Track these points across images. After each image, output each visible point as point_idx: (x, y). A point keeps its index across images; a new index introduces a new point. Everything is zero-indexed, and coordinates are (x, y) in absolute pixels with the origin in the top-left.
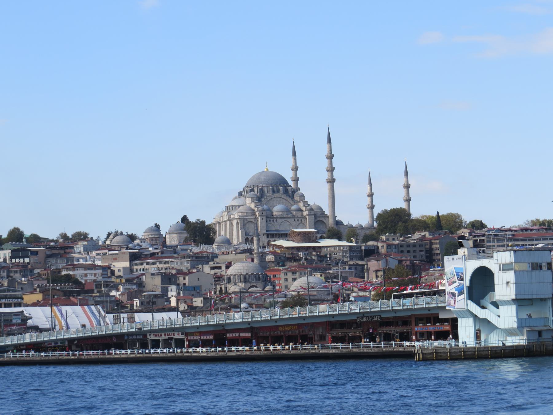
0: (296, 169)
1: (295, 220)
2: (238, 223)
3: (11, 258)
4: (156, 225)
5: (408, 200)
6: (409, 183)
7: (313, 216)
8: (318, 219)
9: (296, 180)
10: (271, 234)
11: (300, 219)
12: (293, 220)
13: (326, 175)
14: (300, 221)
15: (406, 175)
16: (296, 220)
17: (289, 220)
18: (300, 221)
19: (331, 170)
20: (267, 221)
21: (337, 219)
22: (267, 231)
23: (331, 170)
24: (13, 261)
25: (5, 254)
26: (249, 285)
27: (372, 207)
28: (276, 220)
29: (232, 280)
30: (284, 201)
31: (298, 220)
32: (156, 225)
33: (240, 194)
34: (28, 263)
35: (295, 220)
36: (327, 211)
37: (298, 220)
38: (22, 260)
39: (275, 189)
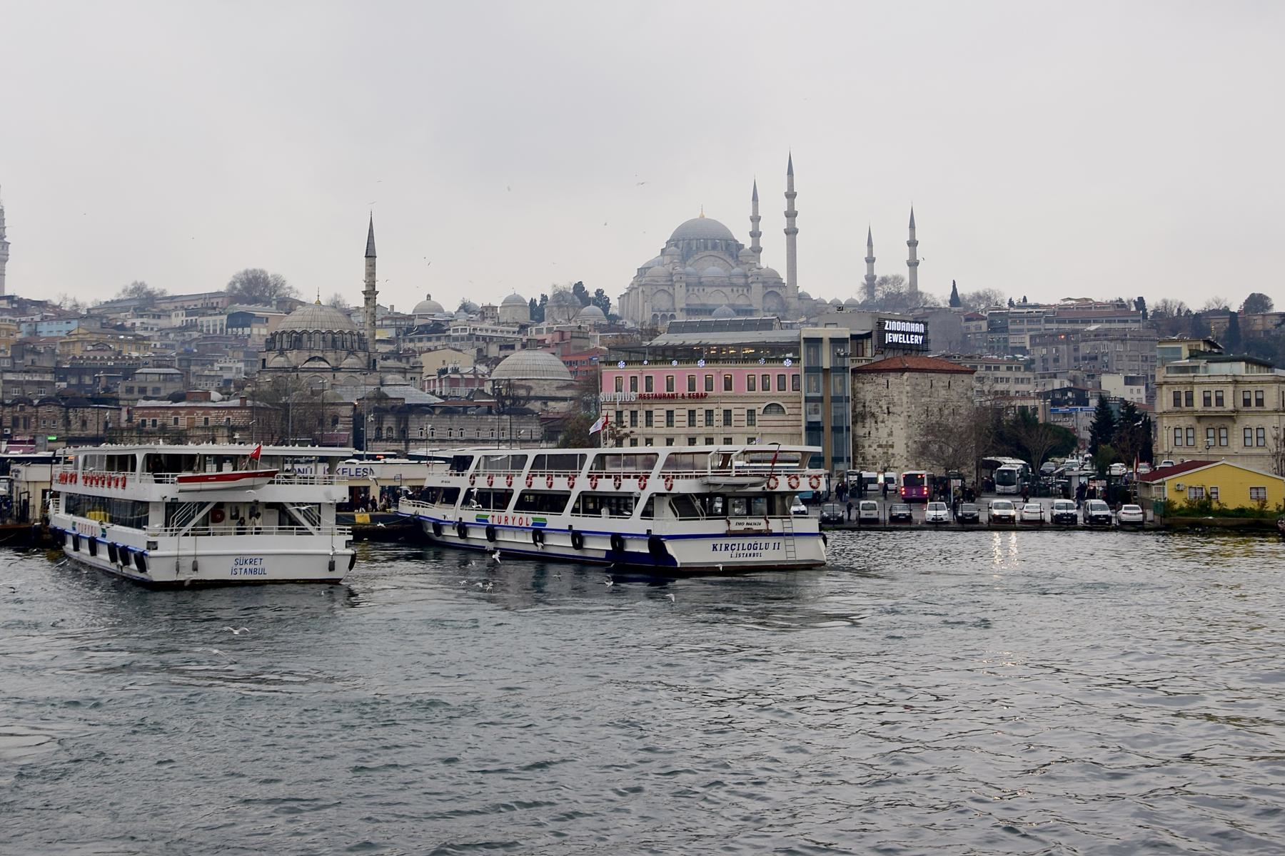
0: (756, 219)
1: (732, 290)
2: (643, 291)
3: (227, 327)
4: (542, 295)
5: (913, 264)
6: (917, 238)
7: (761, 285)
8: (769, 290)
9: (755, 235)
10: (692, 310)
11: (740, 289)
12: (730, 289)
13: (784, 223)
14: (740, 292)
15: (912, 226)
16: (735, 289)
17: (724, 289)
18: (740, 292)
19: (791, 214)
20: (688, 291)
21: (800, 291)
22: (687, 305)
23: (791, 214)
24: (230, 330)
25: (222, 320)
26: (306, 355)
27: (871, 278)
28: (704, 290)
29: (278, 345)
30: (722, 262)
31: (738, 291)
32: (542, 295)
33: (663, 250)
34: (249, 336)
35: (732, 290)
36: (785, 281)
37: (738, 291)
38: (240, 329)
39: (709, 245)
